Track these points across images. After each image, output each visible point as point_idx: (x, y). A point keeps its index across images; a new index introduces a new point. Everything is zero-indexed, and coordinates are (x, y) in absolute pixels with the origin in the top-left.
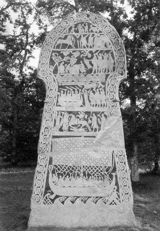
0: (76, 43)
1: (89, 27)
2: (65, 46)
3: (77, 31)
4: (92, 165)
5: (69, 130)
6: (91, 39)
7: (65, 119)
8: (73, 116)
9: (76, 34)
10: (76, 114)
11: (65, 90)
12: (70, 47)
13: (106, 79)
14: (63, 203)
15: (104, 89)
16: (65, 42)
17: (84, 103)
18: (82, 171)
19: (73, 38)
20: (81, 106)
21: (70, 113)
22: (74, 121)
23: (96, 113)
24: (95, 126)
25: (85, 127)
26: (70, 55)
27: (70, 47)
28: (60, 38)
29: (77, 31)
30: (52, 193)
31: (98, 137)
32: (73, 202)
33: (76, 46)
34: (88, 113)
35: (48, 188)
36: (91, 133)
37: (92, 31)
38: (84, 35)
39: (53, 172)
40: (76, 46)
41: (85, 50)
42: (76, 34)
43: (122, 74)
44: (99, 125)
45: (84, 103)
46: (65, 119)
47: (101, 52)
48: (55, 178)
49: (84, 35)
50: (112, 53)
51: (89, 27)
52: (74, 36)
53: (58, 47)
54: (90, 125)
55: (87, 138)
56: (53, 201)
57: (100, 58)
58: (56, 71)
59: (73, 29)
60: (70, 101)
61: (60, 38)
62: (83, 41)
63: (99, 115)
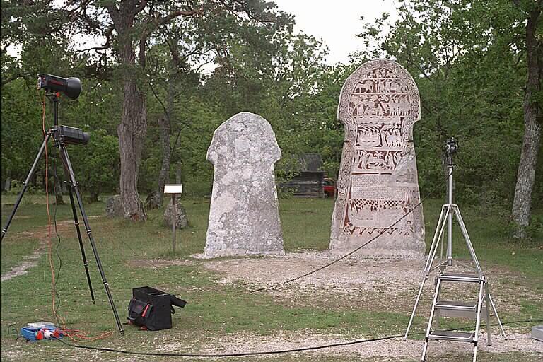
0: (374, 87)
1: (386, 73)
2: (363, 90)
3: (375, 77)
4: (388, 199)
5: (367, 168)
6: (388, 83)
7: (364, 158)
8: (372, 154)
9: (374, 79)
10: (374, 152)
11: (364, 130)
12: (369, 91)
13: (402, 121)
14: (361, 233)
15: (400, 129)
16: (363, 86)
17: (381, 143)
18: (379, 205)
19: (371, 83)
20: (379, 146)
21: (368, 152)
22: (372, 159)
23: (393, 152)
24: (391, 164)
25: (382, 165)
26: (369, 99)
27: (369, 91)
28: (360, 83)
29: (375, 77)
30: (351, 225)
31: (394, 174)
32: (370, 234)
33: (374, 91)
34: (385, 152)
35: (347, 220)
36: (386, 171)
37: (389, 77)
38: (382, 81)
39: (352, 206)
40: (374, 91)
41: (383, 94)
42: (374, 79)
43: (416, 117)
44: (395, 164)
45: (381, 143)
46: (364, 158)
47: (398, 96)
48: (355, 210)
49: (382, 81)
50: (408, 97)
51: (386, 73)
52: (372, 80)
53: (358, 91)
54: (387, 163)
55: (384, 175)
56: (352, 232)
57: (397, 101)
58: (355, 113)
59: (371, 74)
60: (369, 141)
61: (360, 83)
62: (381, 85)
63: (395, 154)
